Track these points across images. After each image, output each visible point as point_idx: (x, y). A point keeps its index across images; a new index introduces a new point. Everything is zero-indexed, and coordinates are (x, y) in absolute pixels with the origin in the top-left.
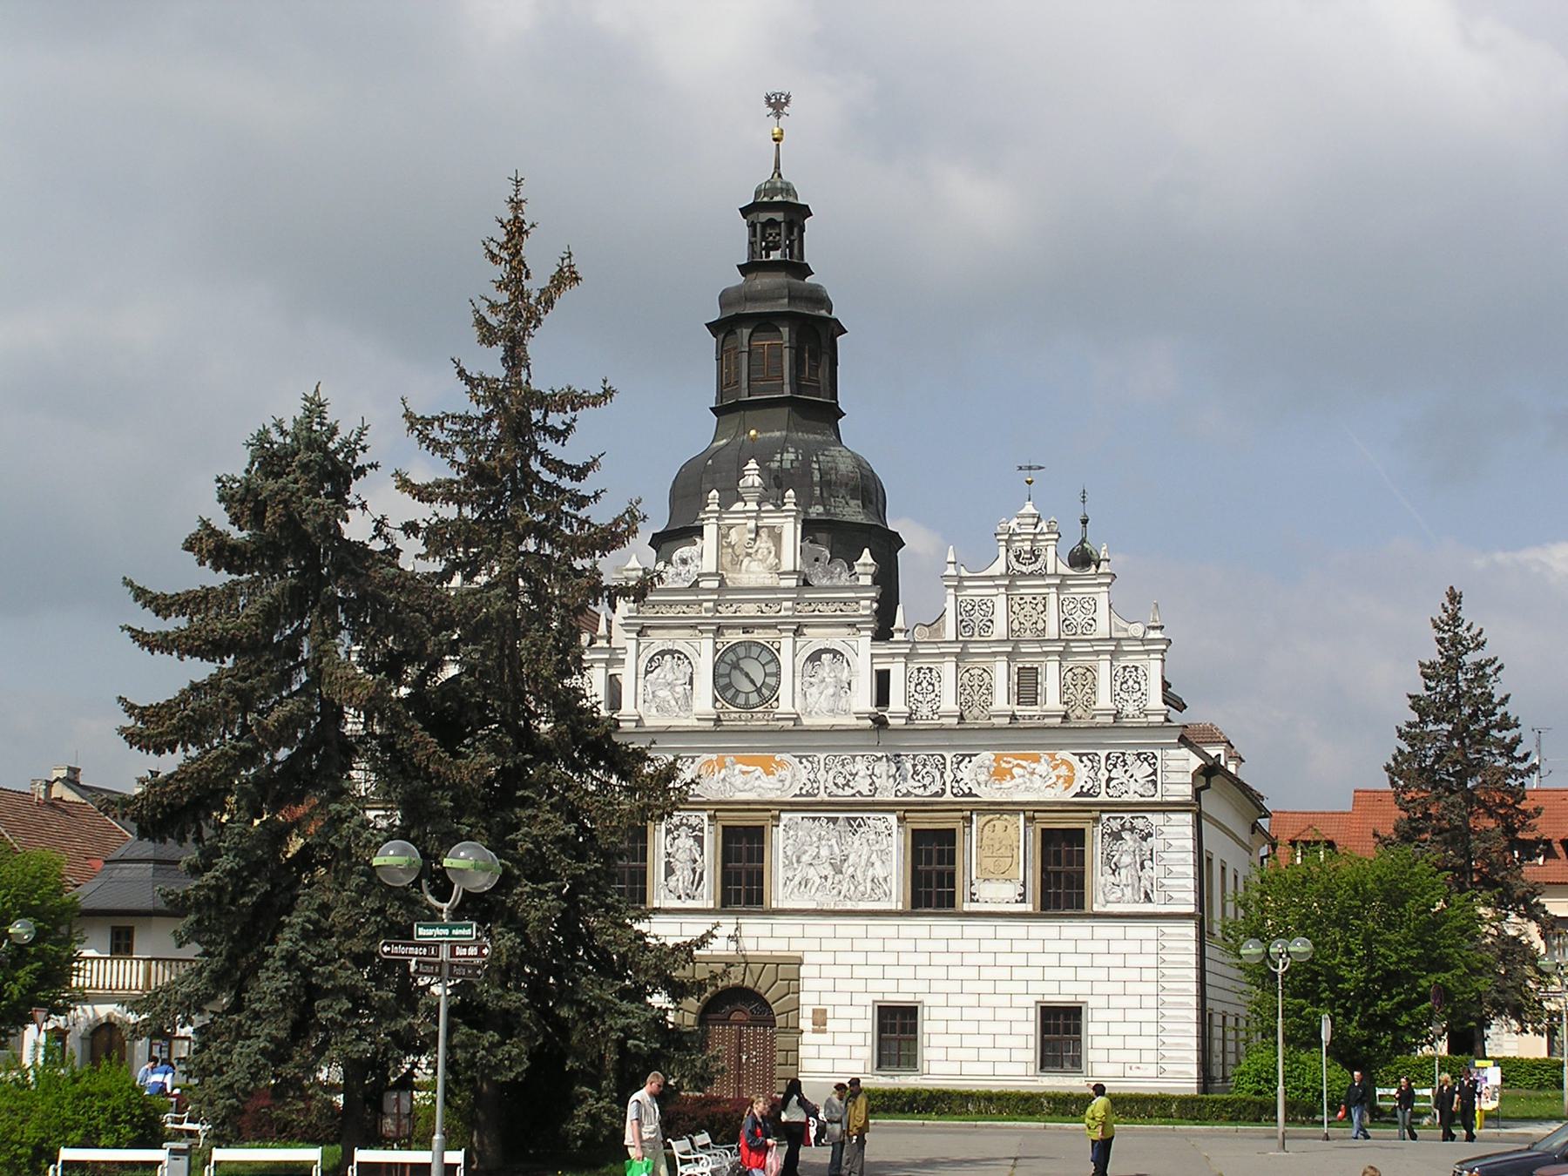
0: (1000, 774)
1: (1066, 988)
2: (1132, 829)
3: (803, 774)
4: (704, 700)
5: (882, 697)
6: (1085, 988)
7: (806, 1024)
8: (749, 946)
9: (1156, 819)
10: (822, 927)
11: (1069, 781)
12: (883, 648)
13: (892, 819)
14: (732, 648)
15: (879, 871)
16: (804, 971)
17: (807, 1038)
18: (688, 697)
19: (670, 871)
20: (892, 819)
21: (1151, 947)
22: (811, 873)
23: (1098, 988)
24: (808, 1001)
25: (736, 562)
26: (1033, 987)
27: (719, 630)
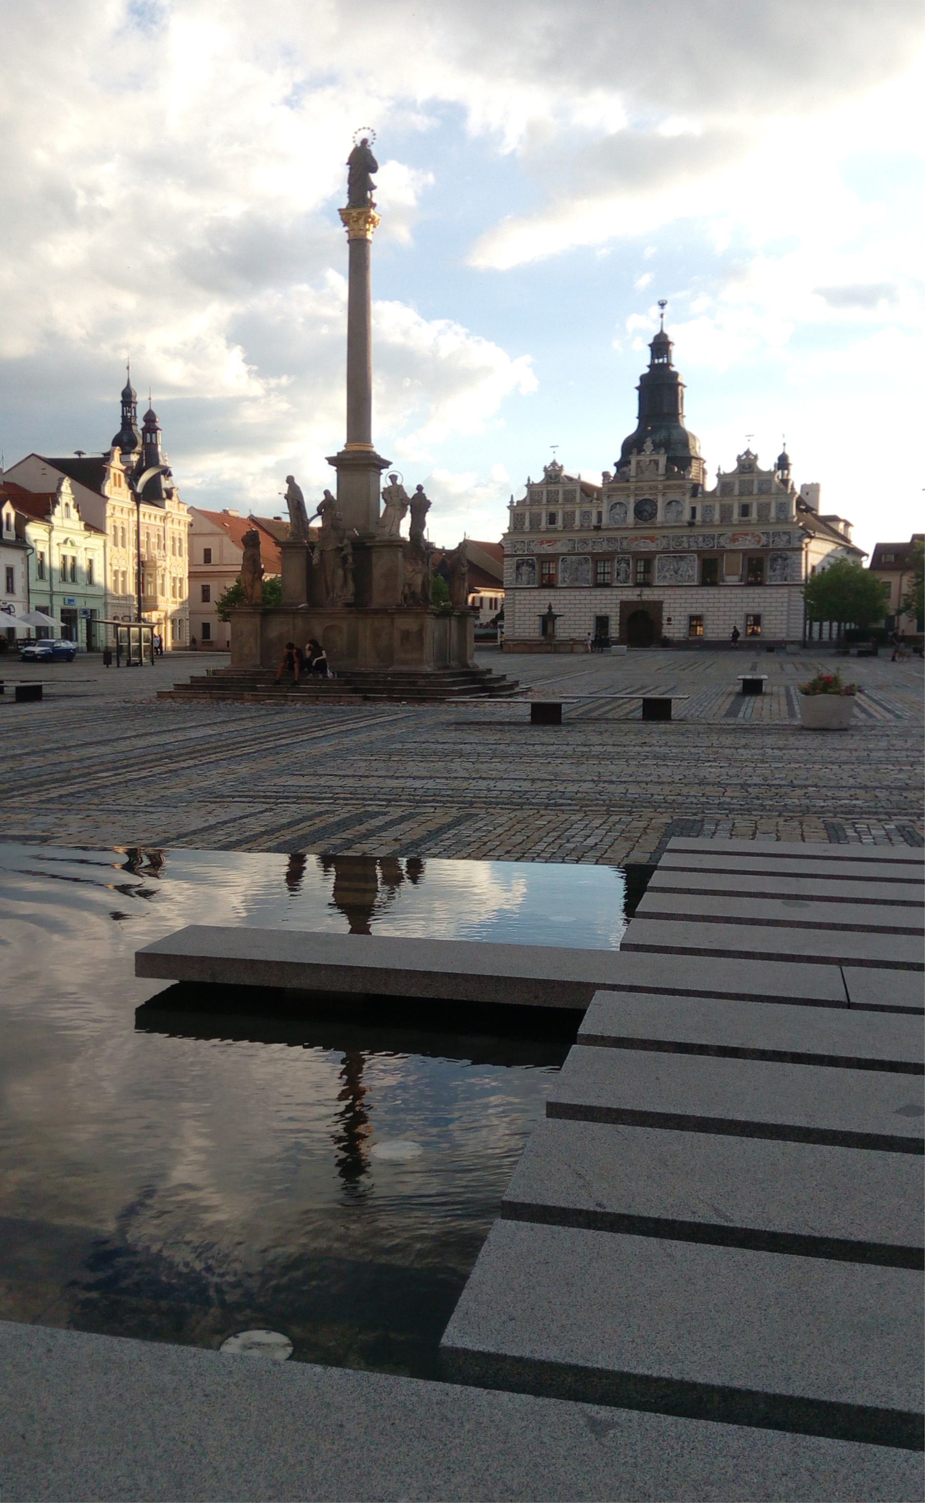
0: (734, 540)
1: (756, 609)
2: (781, 557)
3: (665, 542)
4: (631, 518)
5: (694, 515)
6: (762, 609)
7: (665, 622)
8: (644, 598)
9: (789, 553)
10: (669, 592)
11: (759, 542)
12: (693, 499)
13: (695, 555)
14: (641, 501)
15: (691, 572)
16: (664, 605)
17: (665, 626)
18: (625, 518)
19: (618, 574)
20: (695, 555)
21: (786, 595)
22: (667, 574)
23: (767, 609)
24: (665, 615)
25: (642, 472)
26: (744, 609)
27: (636, 495)
